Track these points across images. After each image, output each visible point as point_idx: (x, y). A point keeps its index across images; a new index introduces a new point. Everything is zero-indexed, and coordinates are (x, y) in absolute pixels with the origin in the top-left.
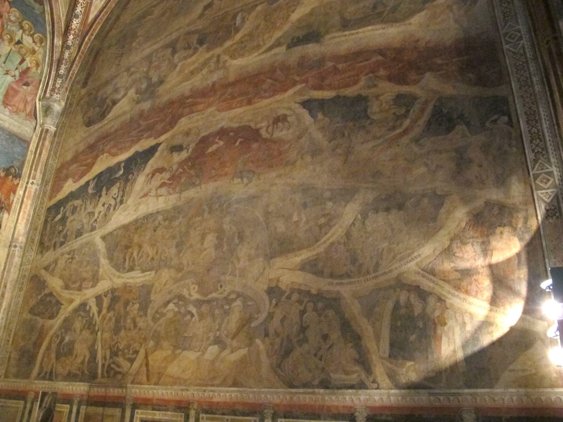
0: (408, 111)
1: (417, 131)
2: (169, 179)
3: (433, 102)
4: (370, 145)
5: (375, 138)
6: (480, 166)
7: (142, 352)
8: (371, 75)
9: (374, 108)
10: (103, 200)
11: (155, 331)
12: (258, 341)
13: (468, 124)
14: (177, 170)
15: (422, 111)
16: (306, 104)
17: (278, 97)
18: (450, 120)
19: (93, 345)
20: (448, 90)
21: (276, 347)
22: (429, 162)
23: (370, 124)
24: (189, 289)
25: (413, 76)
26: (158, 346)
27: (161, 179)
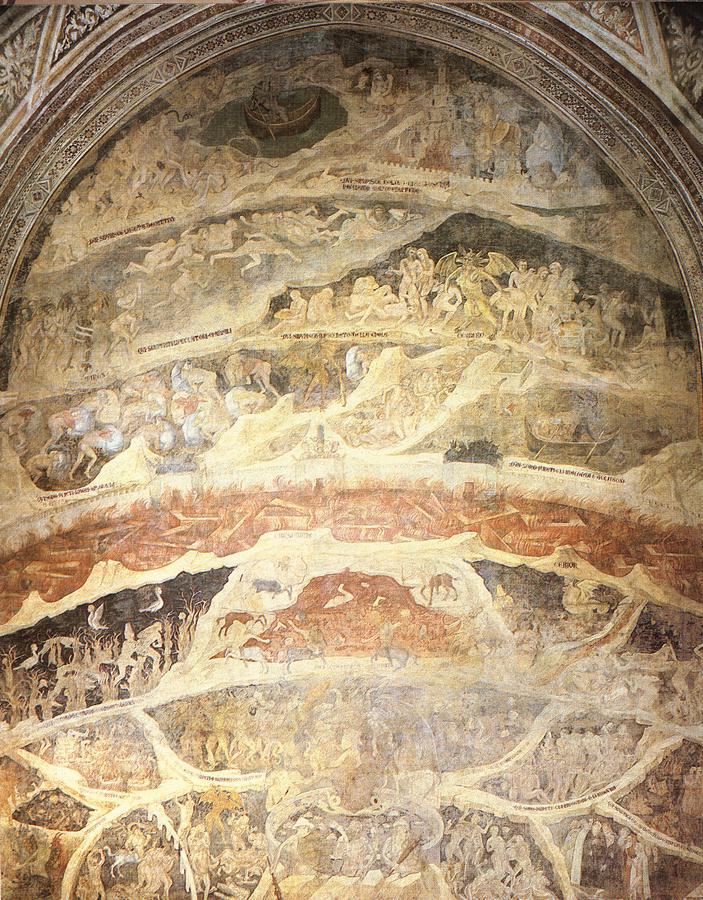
0: (611, 612)
1: (619, 641)
2: (261, 635)
3: (641, 607)
4: (566, 646)
5: (569, 639)
6: (683, 699)
7: (267, 877)
8: (567, 546)
9: (570, 598)
10: (129, 646)
11: (284, 851)
12: (433, 866)
13: (676, 645)
14: (274, 623)
15: (628, 616)
16: (479, 566)
17: (433, 544)
18: (656, 635)
19: (176, 866)
20: (659, 595)
21: (456, 872)
22: (630, 683)
23: (565, 618)
24: (326, 801)
25: (621, 564)
26: (290, 870)
27: (245, 633)
